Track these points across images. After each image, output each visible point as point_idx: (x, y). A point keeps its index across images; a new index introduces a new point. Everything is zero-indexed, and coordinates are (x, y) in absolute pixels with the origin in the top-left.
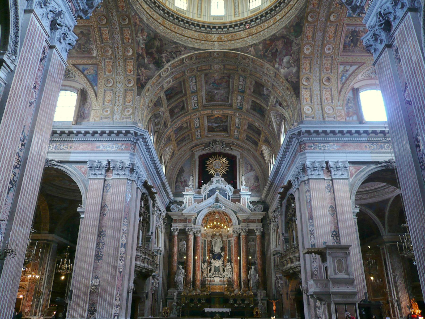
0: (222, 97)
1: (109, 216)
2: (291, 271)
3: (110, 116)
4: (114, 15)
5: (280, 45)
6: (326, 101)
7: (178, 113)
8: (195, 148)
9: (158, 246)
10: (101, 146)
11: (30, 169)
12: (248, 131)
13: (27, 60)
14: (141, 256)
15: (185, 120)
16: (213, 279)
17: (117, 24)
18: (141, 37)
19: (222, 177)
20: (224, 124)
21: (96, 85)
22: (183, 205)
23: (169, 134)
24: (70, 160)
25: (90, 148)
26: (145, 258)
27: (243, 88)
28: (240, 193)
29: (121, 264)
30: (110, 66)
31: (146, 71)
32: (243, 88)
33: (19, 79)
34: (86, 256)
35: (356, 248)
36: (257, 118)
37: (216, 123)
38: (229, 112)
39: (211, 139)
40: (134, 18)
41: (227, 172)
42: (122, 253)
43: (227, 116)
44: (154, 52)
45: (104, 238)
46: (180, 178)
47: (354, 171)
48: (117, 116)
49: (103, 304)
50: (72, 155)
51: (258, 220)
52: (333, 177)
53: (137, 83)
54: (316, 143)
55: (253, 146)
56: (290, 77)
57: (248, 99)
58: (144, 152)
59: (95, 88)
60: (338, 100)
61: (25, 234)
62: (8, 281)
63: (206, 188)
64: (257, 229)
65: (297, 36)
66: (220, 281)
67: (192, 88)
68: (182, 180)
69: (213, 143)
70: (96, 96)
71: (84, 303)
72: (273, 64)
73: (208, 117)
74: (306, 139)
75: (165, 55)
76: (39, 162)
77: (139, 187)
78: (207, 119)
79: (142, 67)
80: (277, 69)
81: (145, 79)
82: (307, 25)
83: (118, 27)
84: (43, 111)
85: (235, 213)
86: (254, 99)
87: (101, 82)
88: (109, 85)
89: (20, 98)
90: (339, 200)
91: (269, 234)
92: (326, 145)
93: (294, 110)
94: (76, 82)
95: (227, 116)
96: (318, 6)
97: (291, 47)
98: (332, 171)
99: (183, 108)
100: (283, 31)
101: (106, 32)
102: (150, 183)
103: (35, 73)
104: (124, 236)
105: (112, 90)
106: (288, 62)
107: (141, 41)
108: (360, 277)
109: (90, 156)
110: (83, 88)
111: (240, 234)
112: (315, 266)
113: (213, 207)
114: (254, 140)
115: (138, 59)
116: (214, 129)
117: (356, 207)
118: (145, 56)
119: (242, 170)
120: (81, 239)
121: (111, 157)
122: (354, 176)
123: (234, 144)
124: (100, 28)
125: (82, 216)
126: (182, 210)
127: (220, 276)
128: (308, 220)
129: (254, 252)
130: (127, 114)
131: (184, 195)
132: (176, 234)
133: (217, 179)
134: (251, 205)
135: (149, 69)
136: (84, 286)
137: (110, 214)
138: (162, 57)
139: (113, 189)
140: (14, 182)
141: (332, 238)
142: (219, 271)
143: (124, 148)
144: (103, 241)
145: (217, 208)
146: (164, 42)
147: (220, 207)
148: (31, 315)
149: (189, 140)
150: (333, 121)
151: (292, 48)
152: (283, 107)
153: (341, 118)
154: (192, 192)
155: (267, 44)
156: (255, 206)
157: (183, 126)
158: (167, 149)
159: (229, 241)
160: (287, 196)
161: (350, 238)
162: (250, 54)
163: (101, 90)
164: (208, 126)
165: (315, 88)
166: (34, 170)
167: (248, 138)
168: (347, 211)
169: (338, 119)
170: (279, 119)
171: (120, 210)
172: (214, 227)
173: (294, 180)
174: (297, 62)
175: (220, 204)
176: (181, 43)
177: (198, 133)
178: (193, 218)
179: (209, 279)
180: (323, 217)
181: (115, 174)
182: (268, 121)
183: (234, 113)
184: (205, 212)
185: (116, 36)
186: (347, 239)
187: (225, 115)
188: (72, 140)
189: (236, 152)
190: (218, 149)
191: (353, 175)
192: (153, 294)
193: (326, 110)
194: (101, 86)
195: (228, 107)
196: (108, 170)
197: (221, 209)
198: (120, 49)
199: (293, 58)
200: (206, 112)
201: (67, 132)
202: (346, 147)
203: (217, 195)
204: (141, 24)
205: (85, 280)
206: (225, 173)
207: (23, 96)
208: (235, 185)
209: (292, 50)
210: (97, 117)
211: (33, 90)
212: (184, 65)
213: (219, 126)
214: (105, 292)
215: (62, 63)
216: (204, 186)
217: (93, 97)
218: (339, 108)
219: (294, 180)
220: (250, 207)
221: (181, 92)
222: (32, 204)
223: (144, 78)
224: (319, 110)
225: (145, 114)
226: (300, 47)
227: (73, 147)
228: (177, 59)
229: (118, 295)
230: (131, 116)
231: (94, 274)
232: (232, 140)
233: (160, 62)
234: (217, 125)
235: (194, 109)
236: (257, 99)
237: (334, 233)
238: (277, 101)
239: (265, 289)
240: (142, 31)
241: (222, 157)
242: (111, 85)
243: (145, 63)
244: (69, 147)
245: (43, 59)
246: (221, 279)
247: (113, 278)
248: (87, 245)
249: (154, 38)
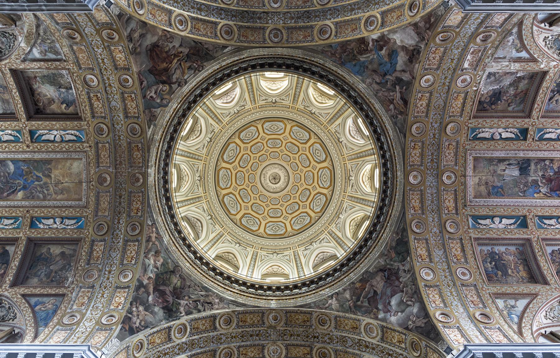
4: (121, 222)
5: (379, 283)
17: (122, 236)
18: (152, 262)
30: (86, 298)
31: (147, 313)
40: (149, 228)
44: (168, 292)
53: (123, 322)
56: (410, 323)
65: (404, 259)
72: (374, 314)
75: (186, 302)
79: (140, 304)
80: (384, 320)
81: (140, 324)
82: (415, 239)
83: (121, 241)
96: (423, 211)
97: (398, 279)
100: (379, 262)
101: (99, 248)
106: (401, 302)
107: (151, 267)
115: (138, 288)
118: (151, 290)
124: (93, 241)
135: (152, 313)
138: (180, 304)
146: (188, 284)
151: (401, 280)
155: (356, 288)
162: (333, 310)
174: (415, 296)
176: (215, 291)
185: (114, 255)
198: (112, 273)
199: (406, 294)
204: (157, 243)
209: (401, 283)
212: (216, 333)
223: (138, 321)
226: (411, 271)
228: (204, 314)
233: (174, 309)
240: (156, 253)
243: (148, 300)
249: (173, 272)
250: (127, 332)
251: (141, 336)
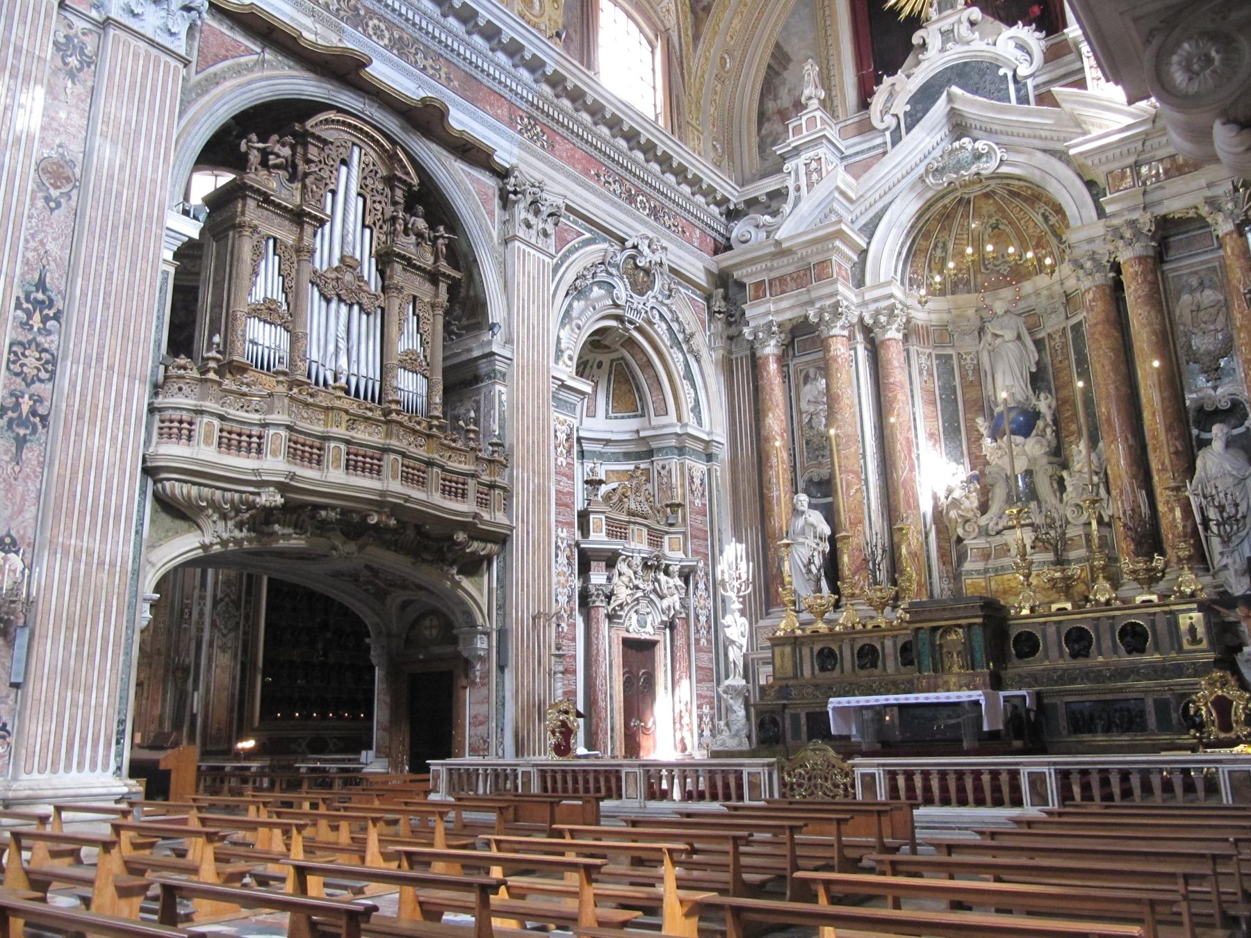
9: (679, 419)
16: (998, 540)
64: (1213, 203)
131: (784, 158)
132: (770, 349)
133: (945, 25)
142: (1032, 494)
145: (959, 167)
147: (978, 156)
159: (1077, 328)
179: (981, 542)
184: (904, 211)
197: (988, 167)
203: (950, 99)
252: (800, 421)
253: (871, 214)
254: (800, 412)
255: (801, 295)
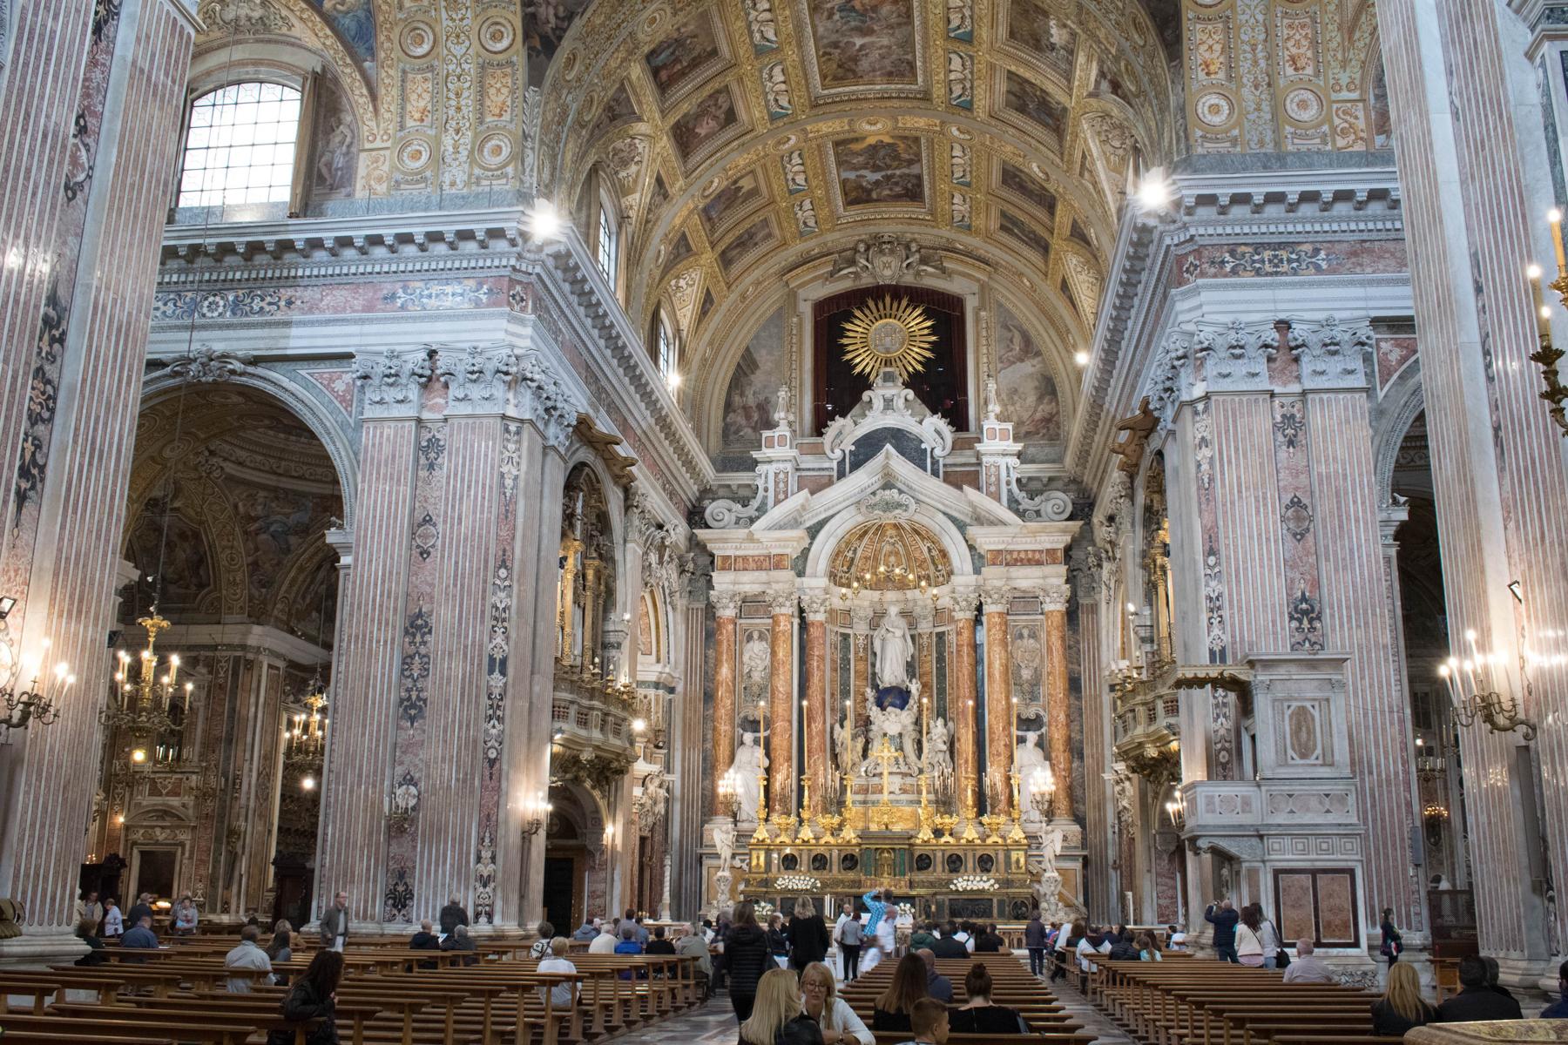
0: (887, 62)
1: (442, 557)
2: (1151, 752)
3: (428, 174)
6: (1290, 71)
7: (708, 136)
8: (799, 270)
10: (400, 293)
11: (87, 423)
12: (1004, 194)
13: (42, 41)
14: (572, 702)
15: (742, 163)
19: (907, 385)
20: (906, 171)
21: (372, 52)
22: (755, 503)
23: (682, 225)
24: (289, 352)
25: (358, 304)
26: (592, 708)
27: (968, 21)
28: (978, 446)
29: (494, 731)
32: (968, 21)
33: (17, 111)
34: (366, 703)
35: (1386, 660)
36: (1033, 142)
37: (876, 169)
38: (921, 122)
39: (864, 232)
41: (927, 363)
42: (496, 692)
43: (917, 140)
45: (427, 638)
46: (742, 395)
47: (1395, 355)
48: (456, 174)
49: (436, 871)
50: (294, 331)
51: (1051, 552)
52: (1308, 385)
53: (527, 36)
54: (1243, 248)
55: (1034, 256)
57: (992, 67)
58: (569, 305)
59: (367, 64)
60: (1344, 64)
61: (93, 641)
62: (47, 794)
63: (847, 431)
66: (903, 790)
67: (757, 36)
68: (751, 401)
69: (868, 249)
70: (373, 96)
71: (368, 869)
73: (837, 144)
74: (1201, 231)
76: (119, 394)
77: (552, 442)
78: (837, 155)
84: (120, 210)
85: (961, 527)
86: (1013, 68)
87: (389, 39)
88: (420, 51)
89: (27, 178)
90: (1329, 476)
91: (1094, 609)
92: (1284, 254)
93: (1161, 111)
94: (293, 45)
95: (917, 140)
98: (1305, 359)
99: (731, 117)
102: (604, 425)
103: (75, 79)
104: (500, 631)
105: (431, 68)
108: (1396, 774)
109: (361, 335)
110: (324, 68)
111: (979, 609)
112: (1222, 732)
113: (873, 506)
114: (1034, 232)
116: (869, 192)
117: (1395, 502)
119: (988, 353)
120: (344, 645)
121: (436, 333)
122: (1395, 376)
123: (954, 250)
125: (345, 560)
126: (752, 520)
127: (904, 769)
128: (1200, 558)
129: (1036, 682)
130: (495, 161)
131: (756, 462)
134: (1020, 495)
136: (365, 810)
137: (443, 551)
139: (450, 454)
140: (35, 471)
141: (1295, 624)
143: (484, 298)
144: (423, 650)
145: (889, 506)
148: (213, 911)
149: (772, 243)
150: (1319, 152)
152: (1124, 97)
153: (1353, 137)
154: (787, 452)
156: (1038, 500)
157: (739, 189)
158: (682, 283)
159: (940, 636)
160: (1145, 463)
161: (1366, 624)
163: (391, 72)
164: (844, 183)
165: (1244, 18)
166: (105, 424)
167: (1009, 225)
168: (1357, 520)
169: (1341, 142)
170: (1117, 144)
171: (480, 537)
172: (879, 585)
173: (1161, 399)
175: (901, 492)
177: (805, 213)
178: (793, 551)
180: (1260, 544)
181: (458, 399)
182: (1078, 155)
183: (943, 123)
186: (1350, 629)
187: (907, 133)
188: (293, 273)
189: (965, 281)
190: (888, 273)
191: (1390, 375)
192: (643, 839)
193: (1292, 108)
194: (387, 57)
195: (916, 103)
196: (429, 380)
200: (825, 127)
201: (270, 247)
202: (1366, 259)
205: (367, 790)
206: (919, 368)
207: (39, 168)
208: (958, 419)
210: (379, 180)
211: (77, 141)
213: (888, 178)
214: (439, 831)
215: (181, 21)
216: (839, 422)
217: (362, 100)
218: (1345, 95)
219: (1161, 399)
220: (1017, 501)
221: (714, 52)
222: (107, 541)
223: (551, 11)
224: (1258, 109)
225: (569, 156)
227: (298, 302)
229: (487, 840)
230: (510, 170)
231: (399, 770)
232: (946, 232)
234: (878, 176)
235: (773, 117)
236: (1027, 64)
237: (1304, 606)
238: (1102, 74)
239: (1079, 819)
241: (904, 303)
242: (426, 47)
244: (282, 303)
245: (106, 22)
246: (909, 780)
247: (465, 781)
248: (369, 666)
250: (542, 56)
251: (566, 46)
252: (741, 671)
253: (815, 520)
254: (742, 663)
255: (762, 576)
